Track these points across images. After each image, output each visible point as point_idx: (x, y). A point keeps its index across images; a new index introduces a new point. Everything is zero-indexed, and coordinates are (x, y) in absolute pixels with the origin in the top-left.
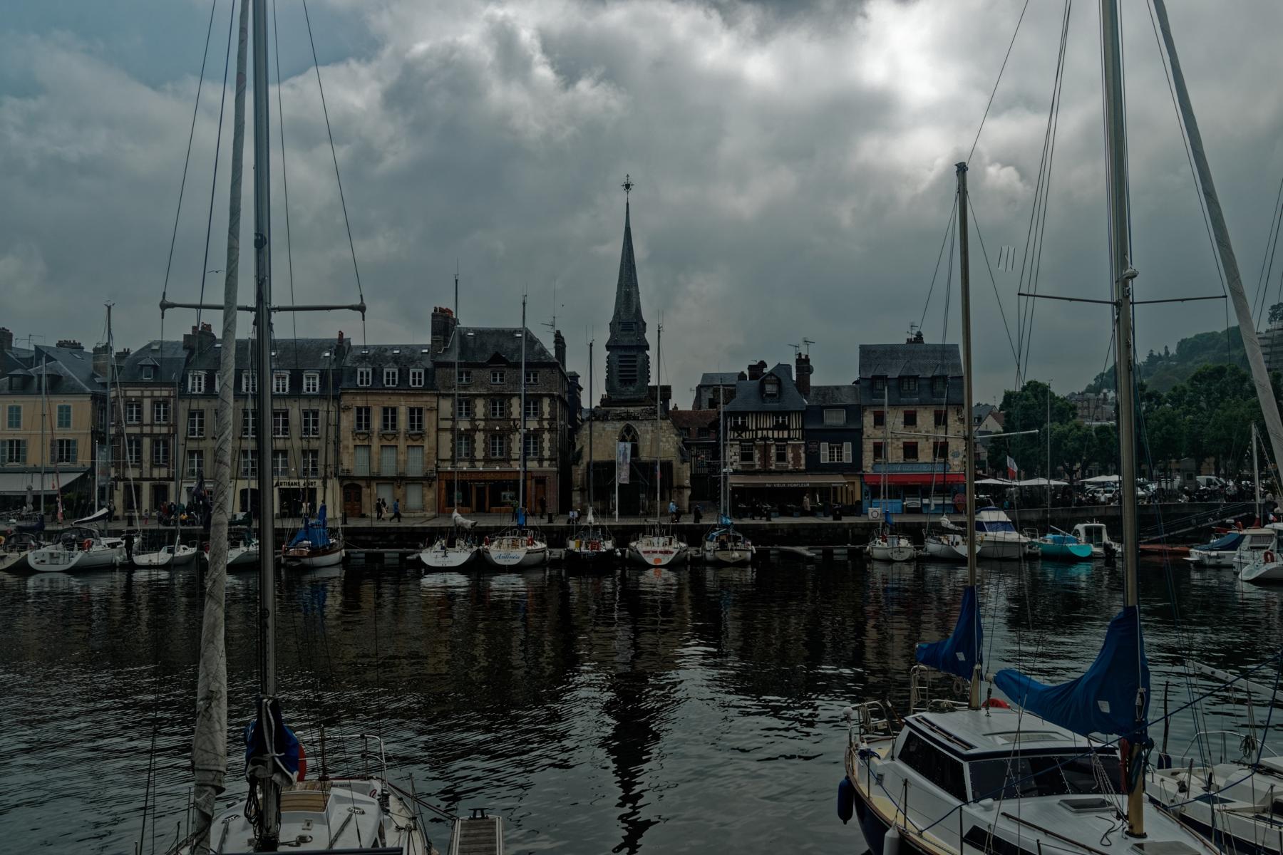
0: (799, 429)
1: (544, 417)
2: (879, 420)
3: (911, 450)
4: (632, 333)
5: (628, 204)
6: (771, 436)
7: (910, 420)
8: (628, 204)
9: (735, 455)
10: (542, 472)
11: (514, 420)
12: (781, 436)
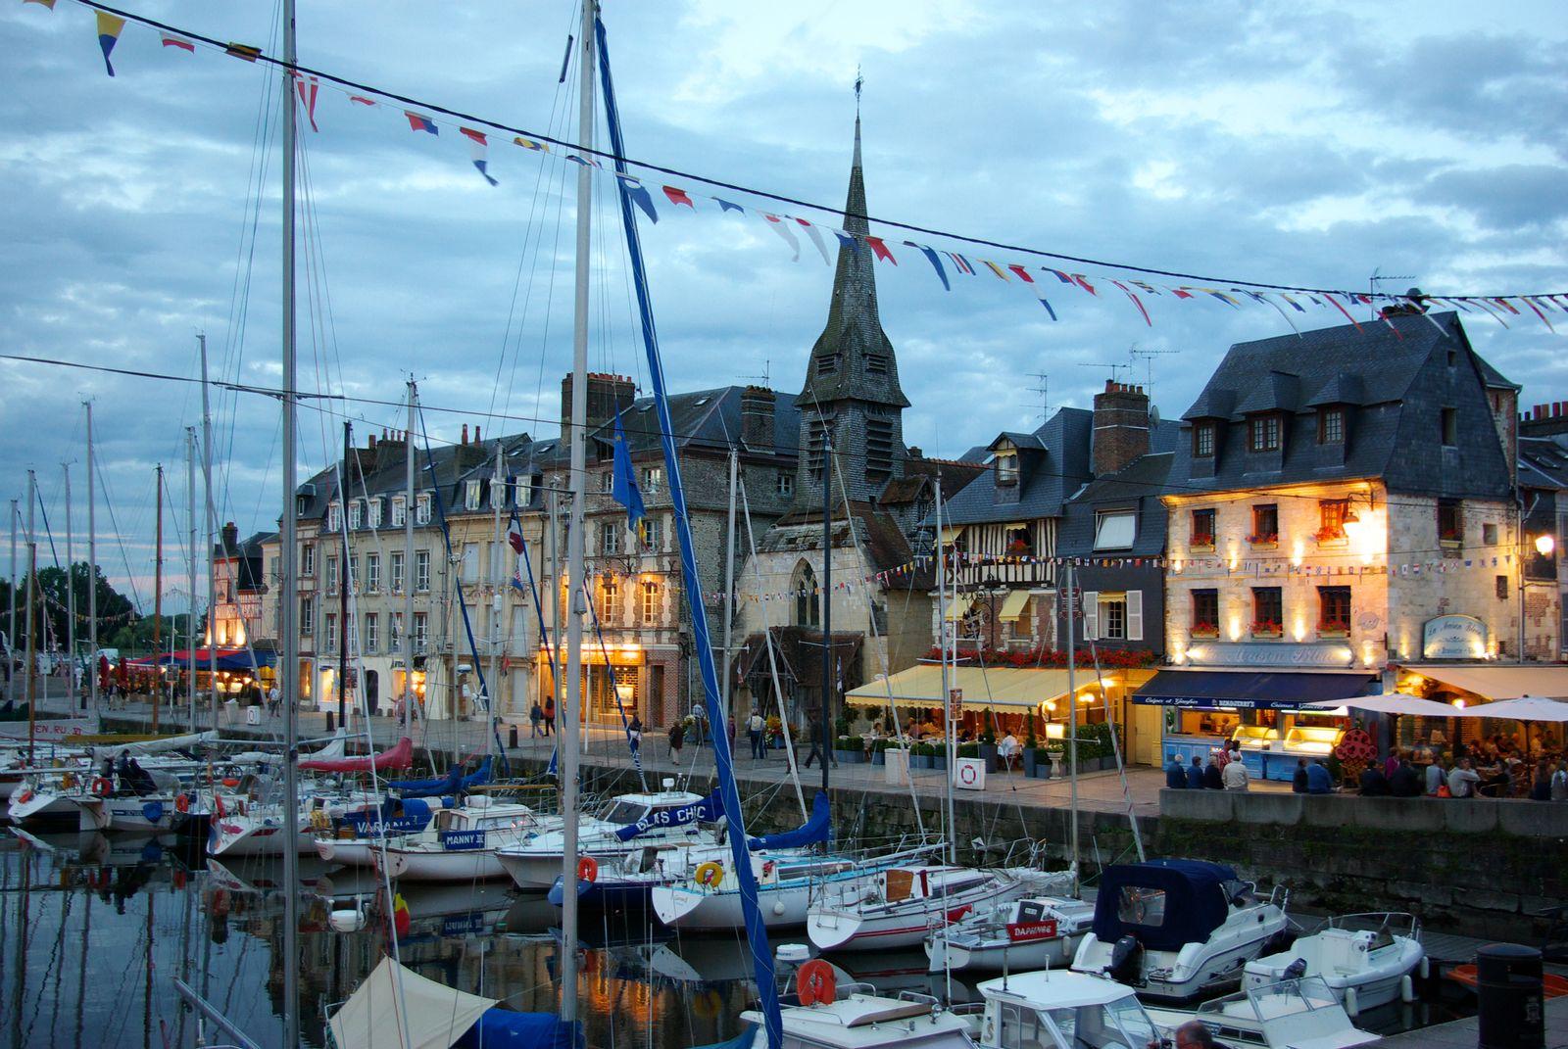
1: (664, 550)
2: (1204, 527)
3: (1268, 606)
4: (834, 375)
5: (858, 122)
6: (1003, 580)
7: (1267, 525)
8: (858, 122)
10: (660, 652)
11: (628, 557)
12: (1028, 578)
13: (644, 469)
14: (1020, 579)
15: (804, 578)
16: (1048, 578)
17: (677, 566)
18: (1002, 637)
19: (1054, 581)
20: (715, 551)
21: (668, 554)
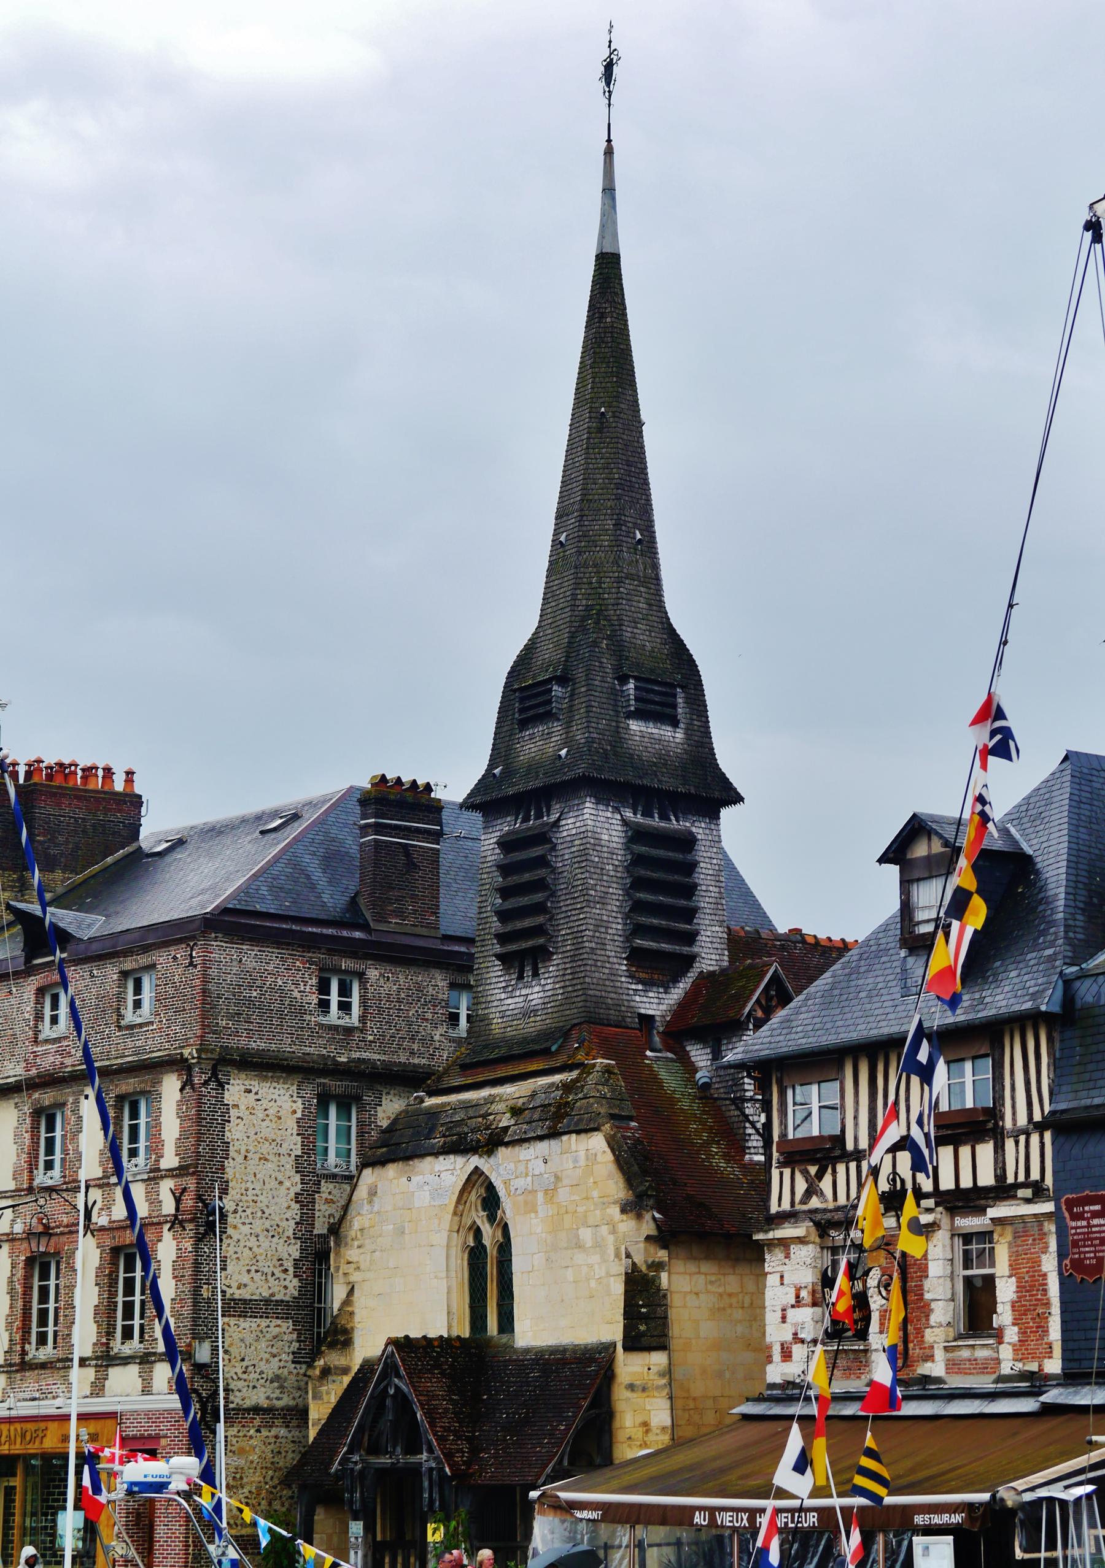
0: (1040, 1127)
5: (609, 152)
8: (609, 152)
9: (798, 1302)
10: (148, 1414)
12: (986, 1178)
13: (125, 974)
14: (966, 1183)
15: (480, 1217)
16: (1035, 1175)
17: (188, 1202)
18: (929, 1336)
19: (1049, 1181)
20: (289, 1163)
21: (171, 1173)
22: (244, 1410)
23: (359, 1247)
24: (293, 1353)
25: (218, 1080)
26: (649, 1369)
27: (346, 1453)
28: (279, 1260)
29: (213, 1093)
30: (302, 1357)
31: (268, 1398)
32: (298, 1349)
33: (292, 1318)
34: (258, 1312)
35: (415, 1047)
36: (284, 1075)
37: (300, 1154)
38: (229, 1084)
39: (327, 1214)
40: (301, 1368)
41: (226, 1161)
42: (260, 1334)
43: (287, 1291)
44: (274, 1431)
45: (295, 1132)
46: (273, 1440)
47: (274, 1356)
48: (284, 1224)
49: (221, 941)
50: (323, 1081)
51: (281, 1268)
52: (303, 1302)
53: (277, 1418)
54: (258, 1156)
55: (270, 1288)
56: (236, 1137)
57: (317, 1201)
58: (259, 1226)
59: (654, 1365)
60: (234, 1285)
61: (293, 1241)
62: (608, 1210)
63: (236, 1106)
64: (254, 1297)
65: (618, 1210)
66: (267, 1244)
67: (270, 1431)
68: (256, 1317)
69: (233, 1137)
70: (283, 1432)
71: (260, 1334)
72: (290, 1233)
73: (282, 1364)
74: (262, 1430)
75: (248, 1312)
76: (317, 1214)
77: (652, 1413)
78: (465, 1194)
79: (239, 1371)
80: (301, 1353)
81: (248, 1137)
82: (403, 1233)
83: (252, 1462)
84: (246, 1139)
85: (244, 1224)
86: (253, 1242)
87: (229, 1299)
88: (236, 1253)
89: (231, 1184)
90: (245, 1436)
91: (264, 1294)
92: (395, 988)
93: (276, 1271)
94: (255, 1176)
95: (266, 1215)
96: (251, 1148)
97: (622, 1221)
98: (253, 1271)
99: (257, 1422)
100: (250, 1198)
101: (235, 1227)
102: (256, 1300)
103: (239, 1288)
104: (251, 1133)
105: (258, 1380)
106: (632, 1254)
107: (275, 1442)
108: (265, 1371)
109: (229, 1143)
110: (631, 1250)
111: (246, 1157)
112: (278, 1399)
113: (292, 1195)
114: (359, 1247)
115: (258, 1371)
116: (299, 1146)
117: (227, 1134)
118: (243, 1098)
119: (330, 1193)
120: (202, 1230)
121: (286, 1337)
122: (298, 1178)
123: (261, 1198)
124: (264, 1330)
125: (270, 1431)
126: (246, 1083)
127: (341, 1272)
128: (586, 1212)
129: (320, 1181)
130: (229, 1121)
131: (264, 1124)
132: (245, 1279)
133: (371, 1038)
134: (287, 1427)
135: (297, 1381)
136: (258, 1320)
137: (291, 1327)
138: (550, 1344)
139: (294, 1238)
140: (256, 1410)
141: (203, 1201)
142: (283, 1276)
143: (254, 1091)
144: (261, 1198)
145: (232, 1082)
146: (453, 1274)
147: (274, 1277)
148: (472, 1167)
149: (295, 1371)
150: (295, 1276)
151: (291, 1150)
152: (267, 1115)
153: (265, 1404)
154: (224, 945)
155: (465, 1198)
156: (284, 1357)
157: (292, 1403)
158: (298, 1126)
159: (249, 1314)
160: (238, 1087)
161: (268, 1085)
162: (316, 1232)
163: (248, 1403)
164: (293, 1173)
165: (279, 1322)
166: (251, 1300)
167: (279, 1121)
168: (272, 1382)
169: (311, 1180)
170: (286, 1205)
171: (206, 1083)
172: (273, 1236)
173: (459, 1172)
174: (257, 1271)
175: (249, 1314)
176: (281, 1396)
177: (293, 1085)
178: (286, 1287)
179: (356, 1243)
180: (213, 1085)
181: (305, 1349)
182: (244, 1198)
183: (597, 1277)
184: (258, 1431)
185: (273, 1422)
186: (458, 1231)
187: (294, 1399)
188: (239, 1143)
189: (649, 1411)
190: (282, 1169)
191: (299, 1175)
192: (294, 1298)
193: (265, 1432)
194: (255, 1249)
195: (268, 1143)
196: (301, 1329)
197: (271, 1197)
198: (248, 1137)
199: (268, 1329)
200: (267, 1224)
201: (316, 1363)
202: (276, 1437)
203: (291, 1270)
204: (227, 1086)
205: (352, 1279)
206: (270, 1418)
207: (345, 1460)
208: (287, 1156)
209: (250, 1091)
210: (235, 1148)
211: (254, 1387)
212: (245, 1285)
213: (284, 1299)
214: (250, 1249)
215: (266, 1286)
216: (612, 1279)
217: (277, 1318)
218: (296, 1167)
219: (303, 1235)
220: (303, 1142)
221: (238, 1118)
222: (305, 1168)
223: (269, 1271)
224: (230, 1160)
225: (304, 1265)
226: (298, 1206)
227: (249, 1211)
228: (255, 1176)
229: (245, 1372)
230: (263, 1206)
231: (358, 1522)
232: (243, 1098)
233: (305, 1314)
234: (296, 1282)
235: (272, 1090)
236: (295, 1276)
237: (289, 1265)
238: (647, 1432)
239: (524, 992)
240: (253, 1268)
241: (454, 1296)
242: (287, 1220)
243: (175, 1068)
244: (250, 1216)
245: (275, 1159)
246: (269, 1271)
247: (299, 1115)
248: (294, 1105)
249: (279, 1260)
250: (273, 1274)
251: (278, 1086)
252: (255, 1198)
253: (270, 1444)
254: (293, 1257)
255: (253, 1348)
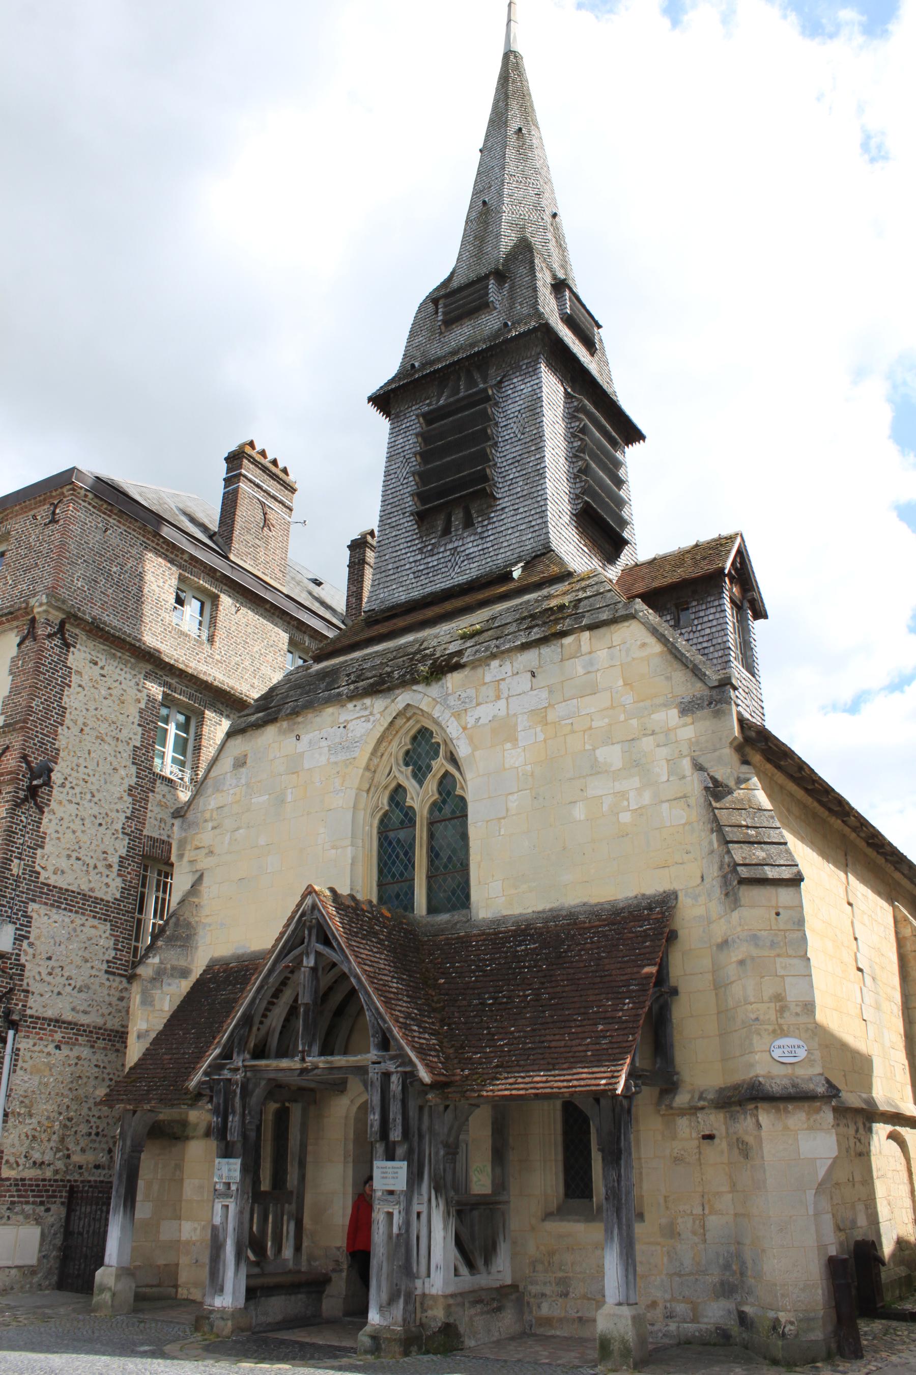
22: (44, 1019)
23: (214, 828)
24: (108, 962)
25: (63, 639)
26: (778, 914)
27: (219, 1056)
28: (104, 852)
29: (57, 650)
30: (117, 968)
31: (73, 1009)
32: (114, 958)
33: (111, 921)
34: (74, 906)
35: (256, 681)
36: (133, 660)
37: (139, 745)
38: (75, 647)
39: (159, 817)
40: (114, 980)
41: (60, 728)
42: (72, 933)
43: (109, 890)
44: (77, 1051)
45: (137, 722)
46: (73, 1062)
47: (87, 961)
48: (113, 815)
49: (90, 504)
50: (169, 680)
51: (105, 862)
52: (125, 906)
53: (82, 1035)
54: (95, 734)
55: (90, 881)
56: (75, 705)
57: (150, 800)
58: (89, 809)
59: (785, 908)
60: (51, 869)
61: (121, 836)
62: (653, 716)
63: (78, 673)
64: (70, 888)
65: (674, 712)
66: (93, 831)
67: (71, 1049)
68: (71, 911)
69: (72, 704)
70: (86, 1052)
71: (72, 933)
72: (119, 826)
73: (94, 972)
74: (63, 1047)
75: (62, 903)
76: (149, 814)
77: (788, 980)
78: (384, 744)
79: (44, 972)
80: (116, 963)
81: (87, 710)
82: (283, 801)
83: (46, 1085)
84: (85, 711)
85: (70, 801)
86: (77, 825)
87: (43, 883)
88: (57, 832)
89: (62, 754)
90: (41, 1051)
91: (83, 887)
92: (244, 620)
93: (99, 865)
94: (89, 753)
95: (95, 799)
96: (89, 722)
97: (685, 725)
98: (74, 857)
99: (58, 1036)
100: (81, 776)
101: (60, 803)
102: (73, 892)
103: (55, 873)
104: (92, 706)
105: (65, 985)
106: (706, 765)
107: (76, 1064)
108: (74, 977)
109: (66, 709)
110: (701, 760)
111: (82, 730)
112: (85, 1012)
113: (126, 787)
114: (214, 828)
115: (66, 974)
116: (139, 737)
117: (65, 698)
118: (87, 668)
119: (164, 796)
120: (22, 794)
121: (102, 942)
122: (133, 769)
123: (92, 779)
124: (79, 929)
125: (71, 1049)
126: (93, 653)
127: (186, 859)
128: (610, 725)
129: (155, 780)
130: (70, 686)
131: (105, 702)
132: (64, 864)
133: (218, 657)
134: (92, 1047)
135: (109, 995)
136: (73, 915)
137: (109, 932)
138: (540, 908)
139: (124, 833)
140: (58, 1022)
141: (28, 763)
142: (107, 872)
143: (100, 664)
144: (92, 779)
145: (78, 646)
146: (360, 843)
147: (96, 871)
148: (401, 706)
149: (107, 983)
150: (119, 875)
151: (130, 739)
152: (111, 695)
153: (68, 1016)
154: (92, 509)
155: (382, 749)
156: (97, 964)
157: (100, 1021)
158: (141, 717)
159: (63, 906)
160: (83, 655)
161: (115, 664)
162: (145, 832)
163: (49, 1013)
164: (129, 763)
165: (96, 922)
166: (67, 890)
167: (122, 705)
168: (80, 991)
169: (146, 776)
170: (119, 796)
171: (50, 636)
172: (100, 825)
173: (378, 716)
174: (78, 859)
175: (63, 906)
176: (89, 1009)
177: (140, 673)
178: (107, 885)
179: (210, 825)
180: (57, 641)
181: (121, 960)
182: (74, 774)
183: (633, 806)
184: (58, 1047)
185: (77, 1040)
186: (368, 791)
187: (103, 1015)
188: (77, 712)
189: (782, 977)
190: (119, 755)
191: (135, 767)
192: (116, 899)
193: (65, 1051)
194: (79, 833)
195: (107, 725)
196: (119, 936)
197: (103, 781)
198: (87, 710)
199: (82, 928)
200: (95, 810)
201: (150, 961)
202: (79, 1058)
203: (116, 867)
204: (72, 649)
205: (200, 866)
206: (74, 1034)
207: (216, 1067)
208: (125, 744)
209: (96, 664)
210: (72, 717)
211: (59, 993)
212: (63, 872)
213: (104, 897)
214: (74, 832)
215: (85, 879)
216: (665, 806)
217: (95, 917)
218: (134, 758)
219: (132, 832)
220: (143, 734)
221: (80, 686)
222: (142, 762)
223: (92, 862)
224: (64, 727)
225: (129, 864)
226: (130, 799)
227: (78, 790)
228: (89, 753)
229: (50, 974)
230: (94, 788)
231: (231, 1160)
232: (87, 668)
233: (125, 920)
234: (119, 880)
235: (118, 670)
236: (119, 875)
237: (114, 860)
238: (782, 1010)
239: (450, 546)
240: (74, 855)
241: (360, 869)
242: (118, 811)
243: (15, 623)
244: (78, 796)
245: (113, 743)
246: (92, 862)
247: (143, 705)
248: (139, 695)
249: (104, 852)
250: (95, 867)
251: (125, 669)
252: (86, 777)
253: (70, 1065)
254: (119, 853)
255: (63, 946)
